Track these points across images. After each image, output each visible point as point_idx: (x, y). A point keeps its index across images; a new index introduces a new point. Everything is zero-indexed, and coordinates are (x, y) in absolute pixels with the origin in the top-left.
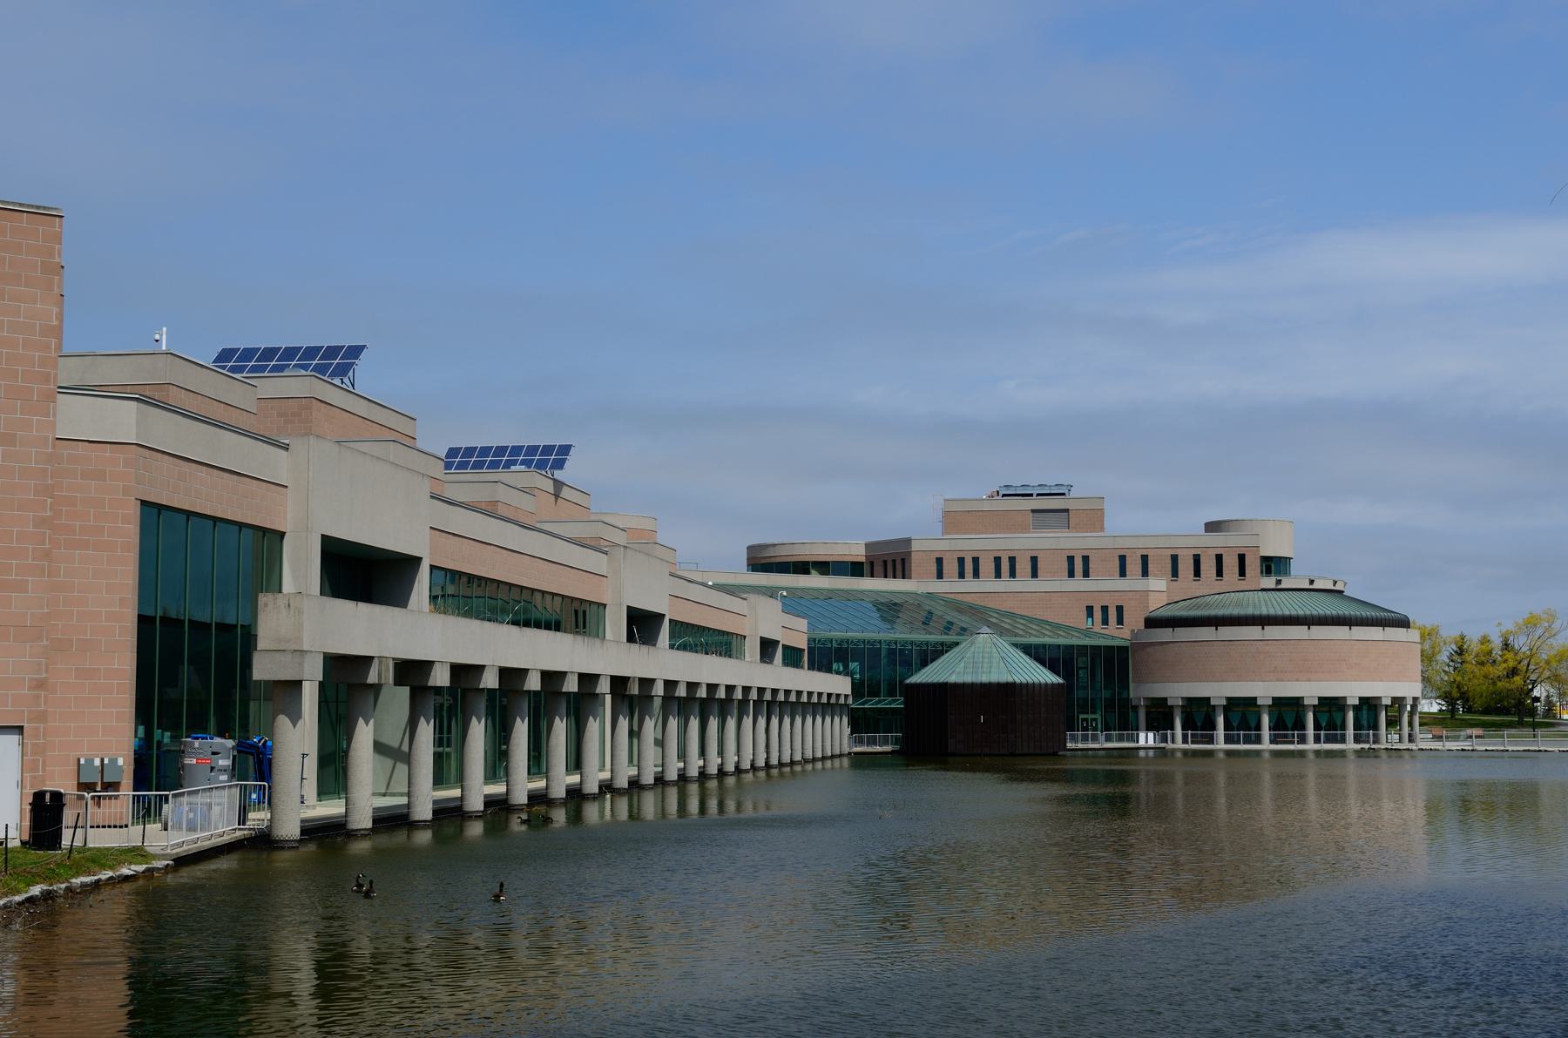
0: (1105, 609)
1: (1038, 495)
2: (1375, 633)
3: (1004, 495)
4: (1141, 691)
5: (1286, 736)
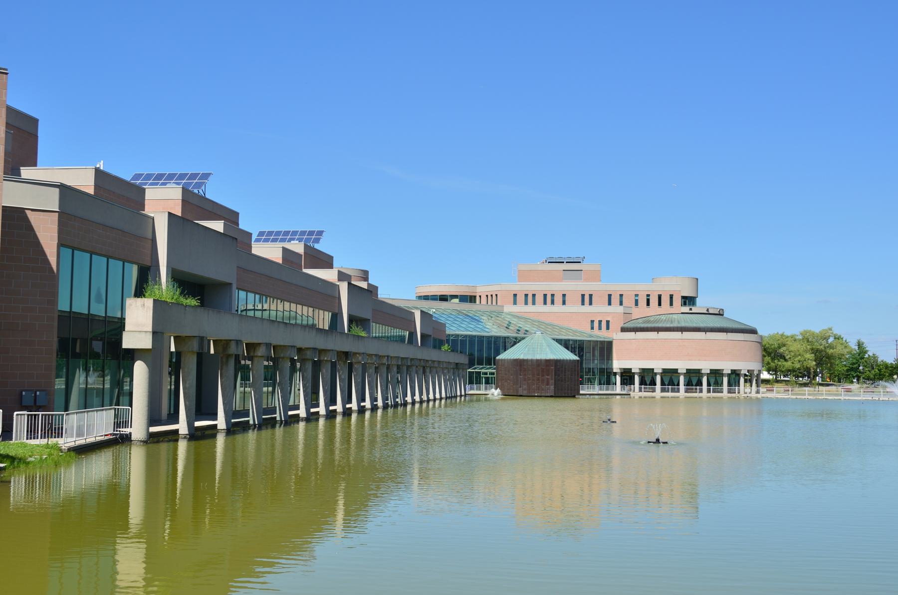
1: (567, 262)
3: (549, 262)
4: (617, 365)
5: (692, 389)
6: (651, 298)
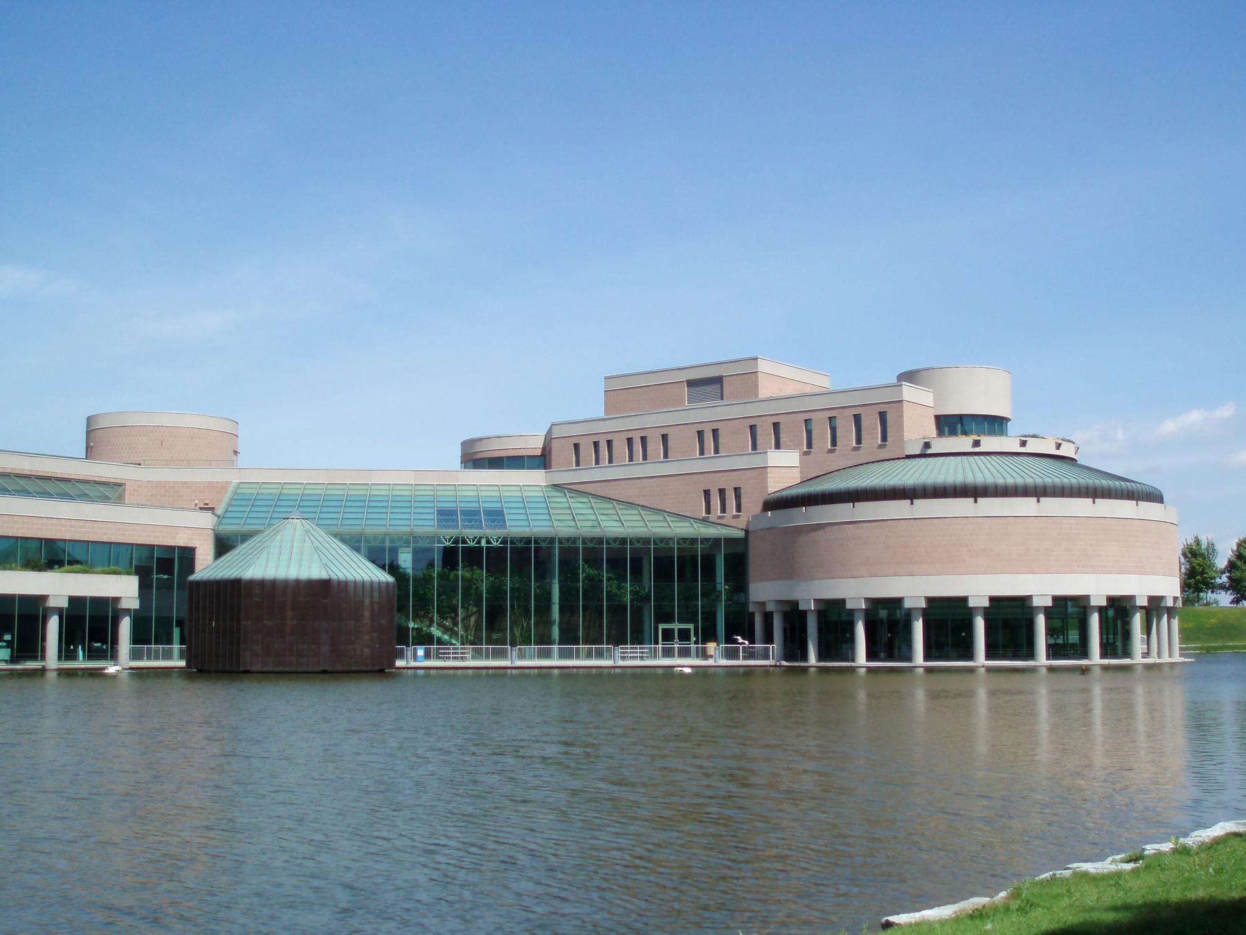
0: (722, 492)
2: (1081, 507)
6: (839, 424)
